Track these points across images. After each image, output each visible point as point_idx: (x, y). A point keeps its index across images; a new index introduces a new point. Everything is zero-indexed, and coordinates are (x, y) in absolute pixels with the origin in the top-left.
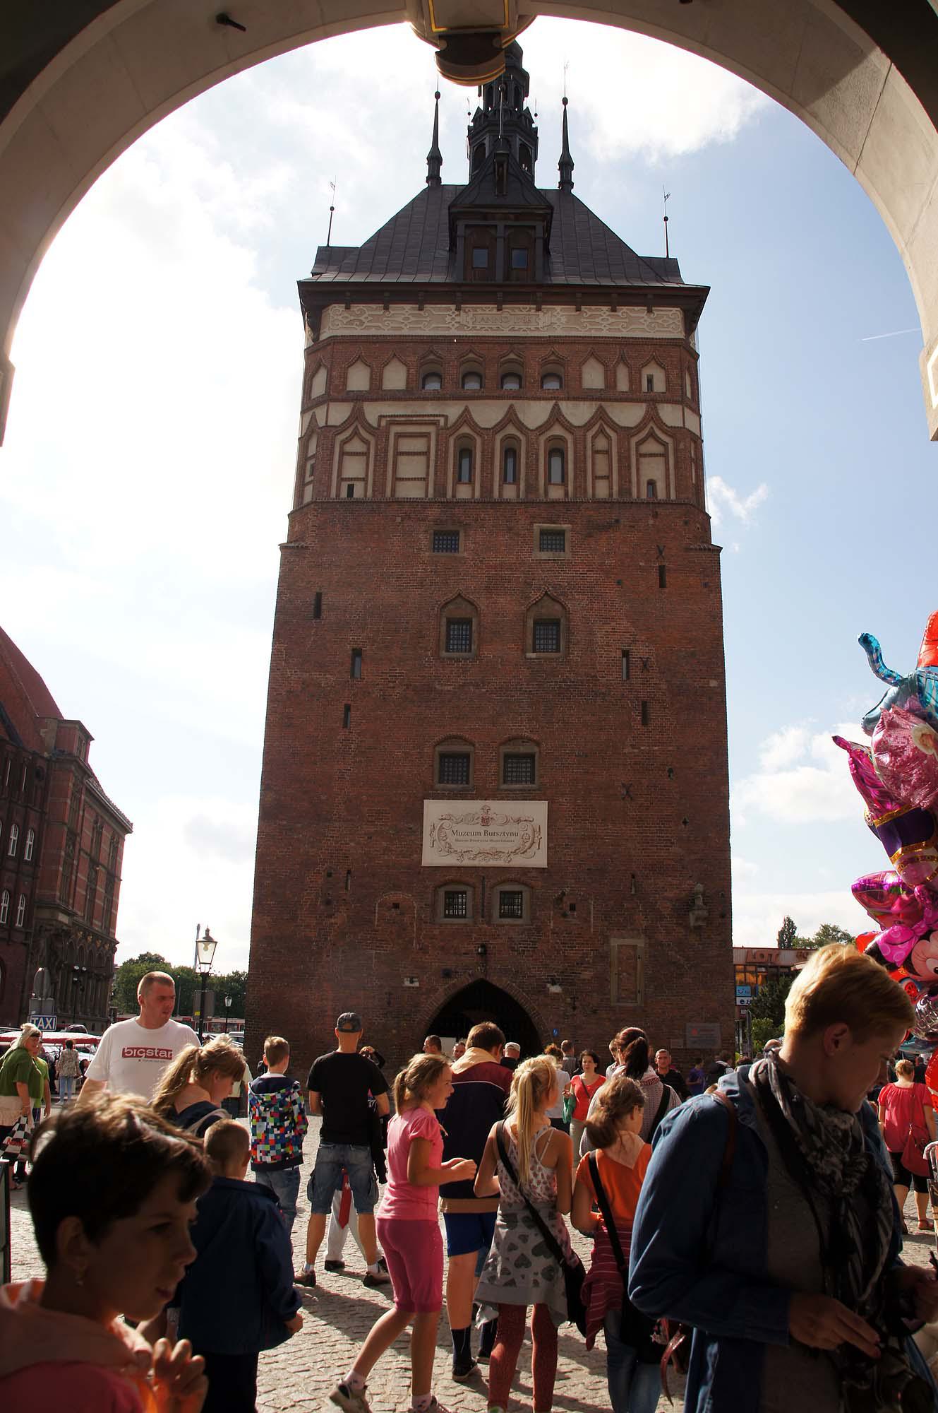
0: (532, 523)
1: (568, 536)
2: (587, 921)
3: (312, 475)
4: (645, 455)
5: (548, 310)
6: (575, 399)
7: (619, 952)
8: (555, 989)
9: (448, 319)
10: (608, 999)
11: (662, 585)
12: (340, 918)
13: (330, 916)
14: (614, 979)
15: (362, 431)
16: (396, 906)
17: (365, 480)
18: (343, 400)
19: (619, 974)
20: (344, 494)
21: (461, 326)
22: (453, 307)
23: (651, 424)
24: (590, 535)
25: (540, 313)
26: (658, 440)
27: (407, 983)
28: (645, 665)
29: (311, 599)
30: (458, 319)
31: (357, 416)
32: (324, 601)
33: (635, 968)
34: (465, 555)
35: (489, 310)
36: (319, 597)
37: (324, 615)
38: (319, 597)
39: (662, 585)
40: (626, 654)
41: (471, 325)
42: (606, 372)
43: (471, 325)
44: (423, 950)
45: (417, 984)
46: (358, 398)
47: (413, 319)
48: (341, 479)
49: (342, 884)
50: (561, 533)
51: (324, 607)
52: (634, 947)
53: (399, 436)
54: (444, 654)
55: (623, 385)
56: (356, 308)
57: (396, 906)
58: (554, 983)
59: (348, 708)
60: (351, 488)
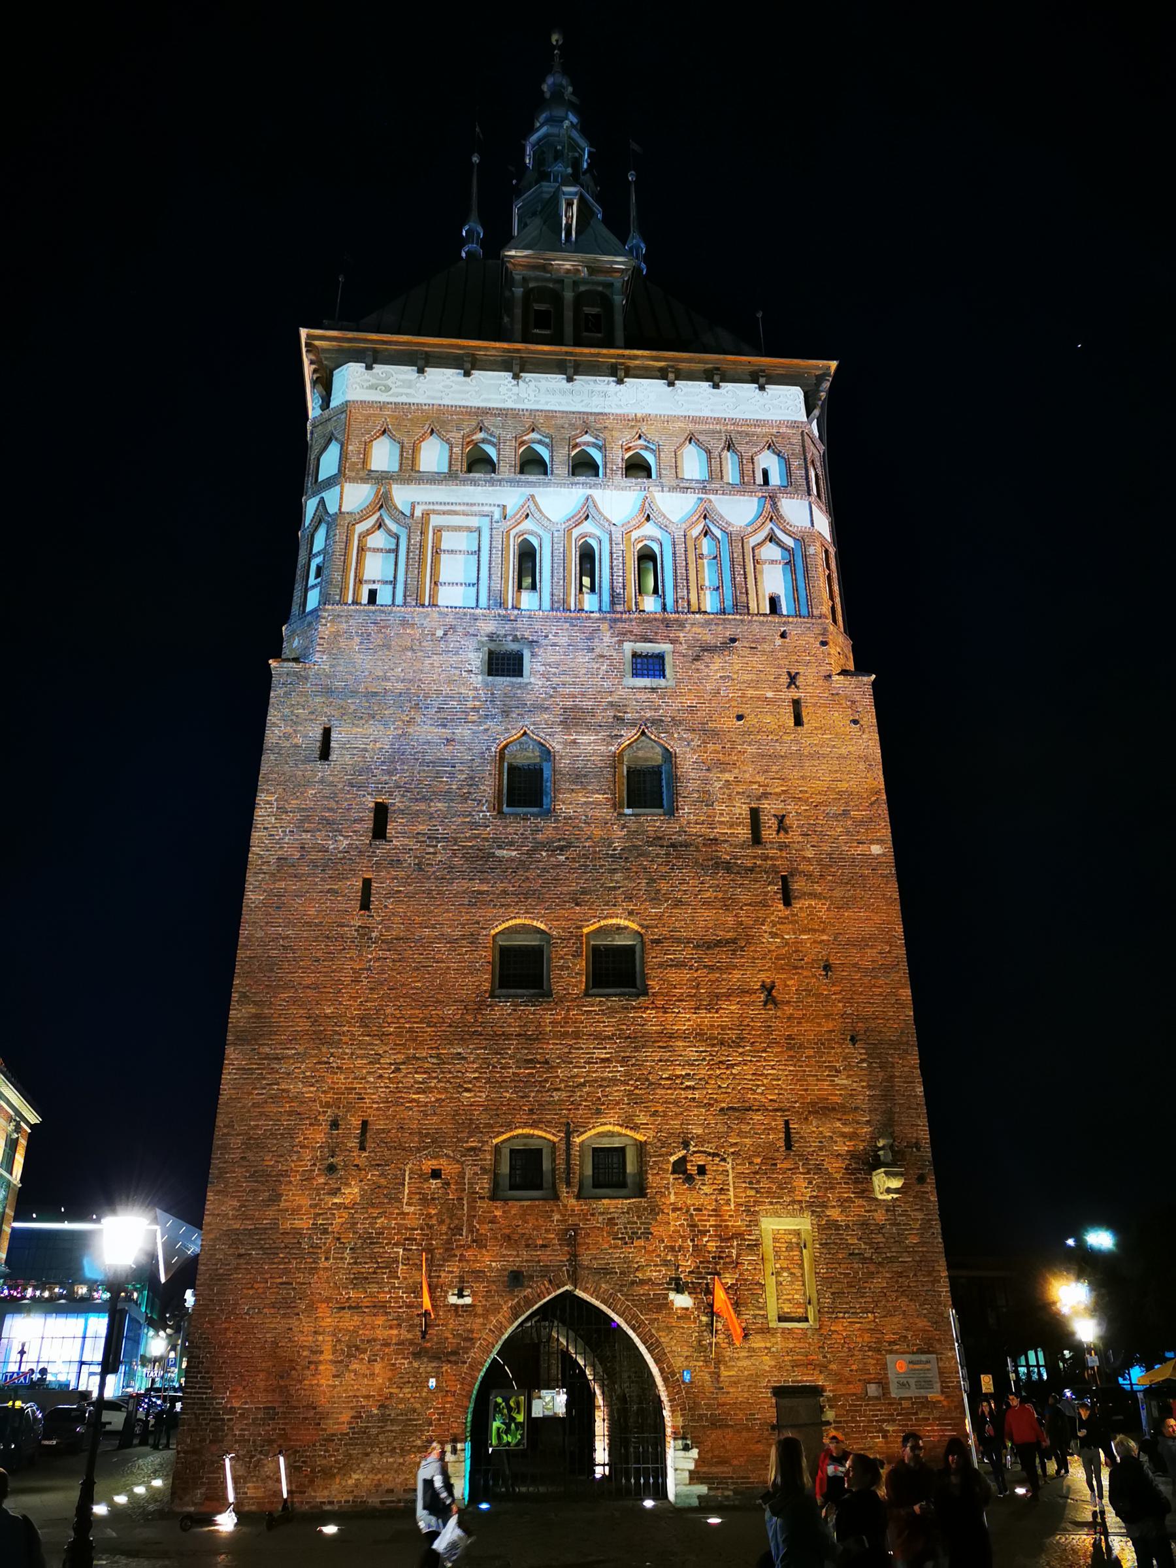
0: (621, 642)
1: (668, 660)
2: (722, 1191)
3: (318, 575)
6: (672, 489)
7: (775, 1240)
8: (682, 1301)
9: (503, 389)
10: (765, 1317)
11: (798, 721)
12: (352, 1192)
13: (335, 1192)
14: (770, 1282)
15: (389, 522)
16: (436, 1174)
17: (394, 583)
18: (364, 480)
19: (778, 1274)
20: (365, 600)
21: (519, 399)
22: (508, 375)
24: (697, 658)
26: (779, 543)
27: (453, 1300)
28: (782, 824)
29: (317, 733)
30: (515, 389)
31: (383, 502)
32: (334, 735)
33: (801, 1267)
35: (556, 381)
36: (327, 732)
37: (333, 757)
38: (327, 732)
39: (798, 721)
40: (755, 813)
41: (532, 398)
42: (710, 459)
43: (532, 398)
44: (480, 1243)
45: (468, 1300)
46: (382, 479)
47: (455, 387)
48: (359, 581)
49: (353, 1143)
50: (660, 658)
51: (333, 744)
52: (797, 1233)
53: (438, 530)
54: (505, 809)
55: (731, 473)
56: (379, 368)
57: (436, 1174)
58: (679, 1290)
59: (367, 883)
60: (373, 594)
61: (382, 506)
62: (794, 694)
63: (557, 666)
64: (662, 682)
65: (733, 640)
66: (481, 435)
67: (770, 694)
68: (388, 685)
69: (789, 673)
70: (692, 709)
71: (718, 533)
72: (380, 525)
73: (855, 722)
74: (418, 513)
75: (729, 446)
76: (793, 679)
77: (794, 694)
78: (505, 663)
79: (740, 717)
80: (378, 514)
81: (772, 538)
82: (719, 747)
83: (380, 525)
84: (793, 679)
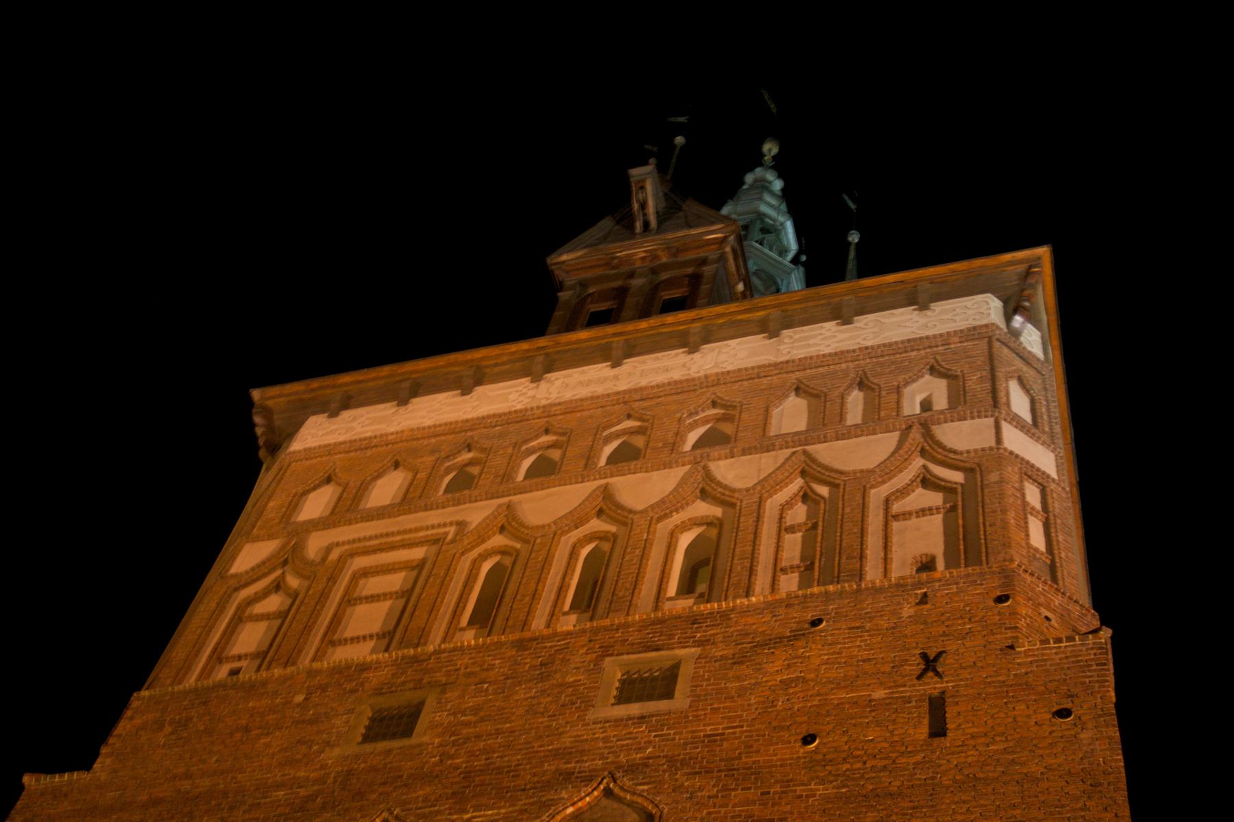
4: (906, 515)
5: (713, 350)
23: (918, 462)
25: (697, 356)
34: (426, 739)
61: (285, 562)
62: (933, 686)
63: (476, 710)
64: (663, 705)
65: (816, 623)
66: (467, 456)
67: (879, 694)
68: (186, 785)
69: (924, 656)
70: (712, 739)
71: (824, 491)
72: (277, 586)
73: (1063, 713)
74: (334, 556)
75: (861, 385)
76: (930, 664)
77: (933, 686)
78: (394, 723)
79: (808, 739)
80: (278, 572)
81: (928, 482)
82: (753, 794)
83: (277, 586)
84: (930, 664)
